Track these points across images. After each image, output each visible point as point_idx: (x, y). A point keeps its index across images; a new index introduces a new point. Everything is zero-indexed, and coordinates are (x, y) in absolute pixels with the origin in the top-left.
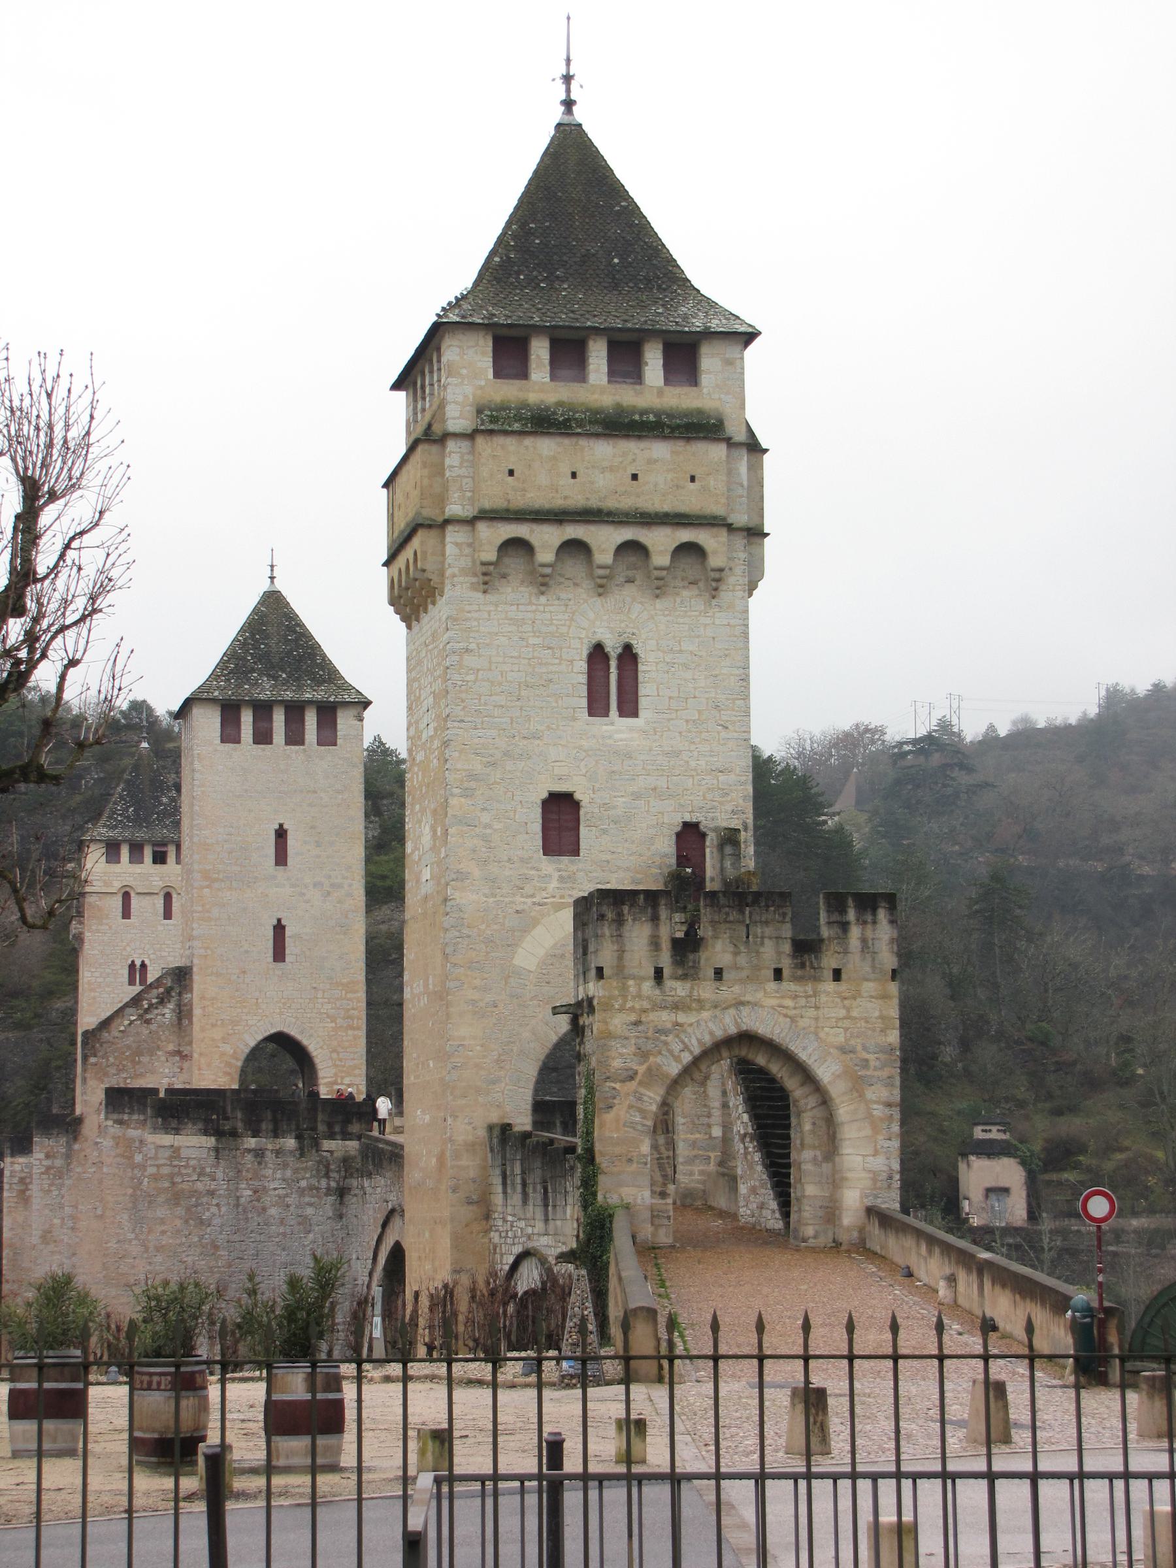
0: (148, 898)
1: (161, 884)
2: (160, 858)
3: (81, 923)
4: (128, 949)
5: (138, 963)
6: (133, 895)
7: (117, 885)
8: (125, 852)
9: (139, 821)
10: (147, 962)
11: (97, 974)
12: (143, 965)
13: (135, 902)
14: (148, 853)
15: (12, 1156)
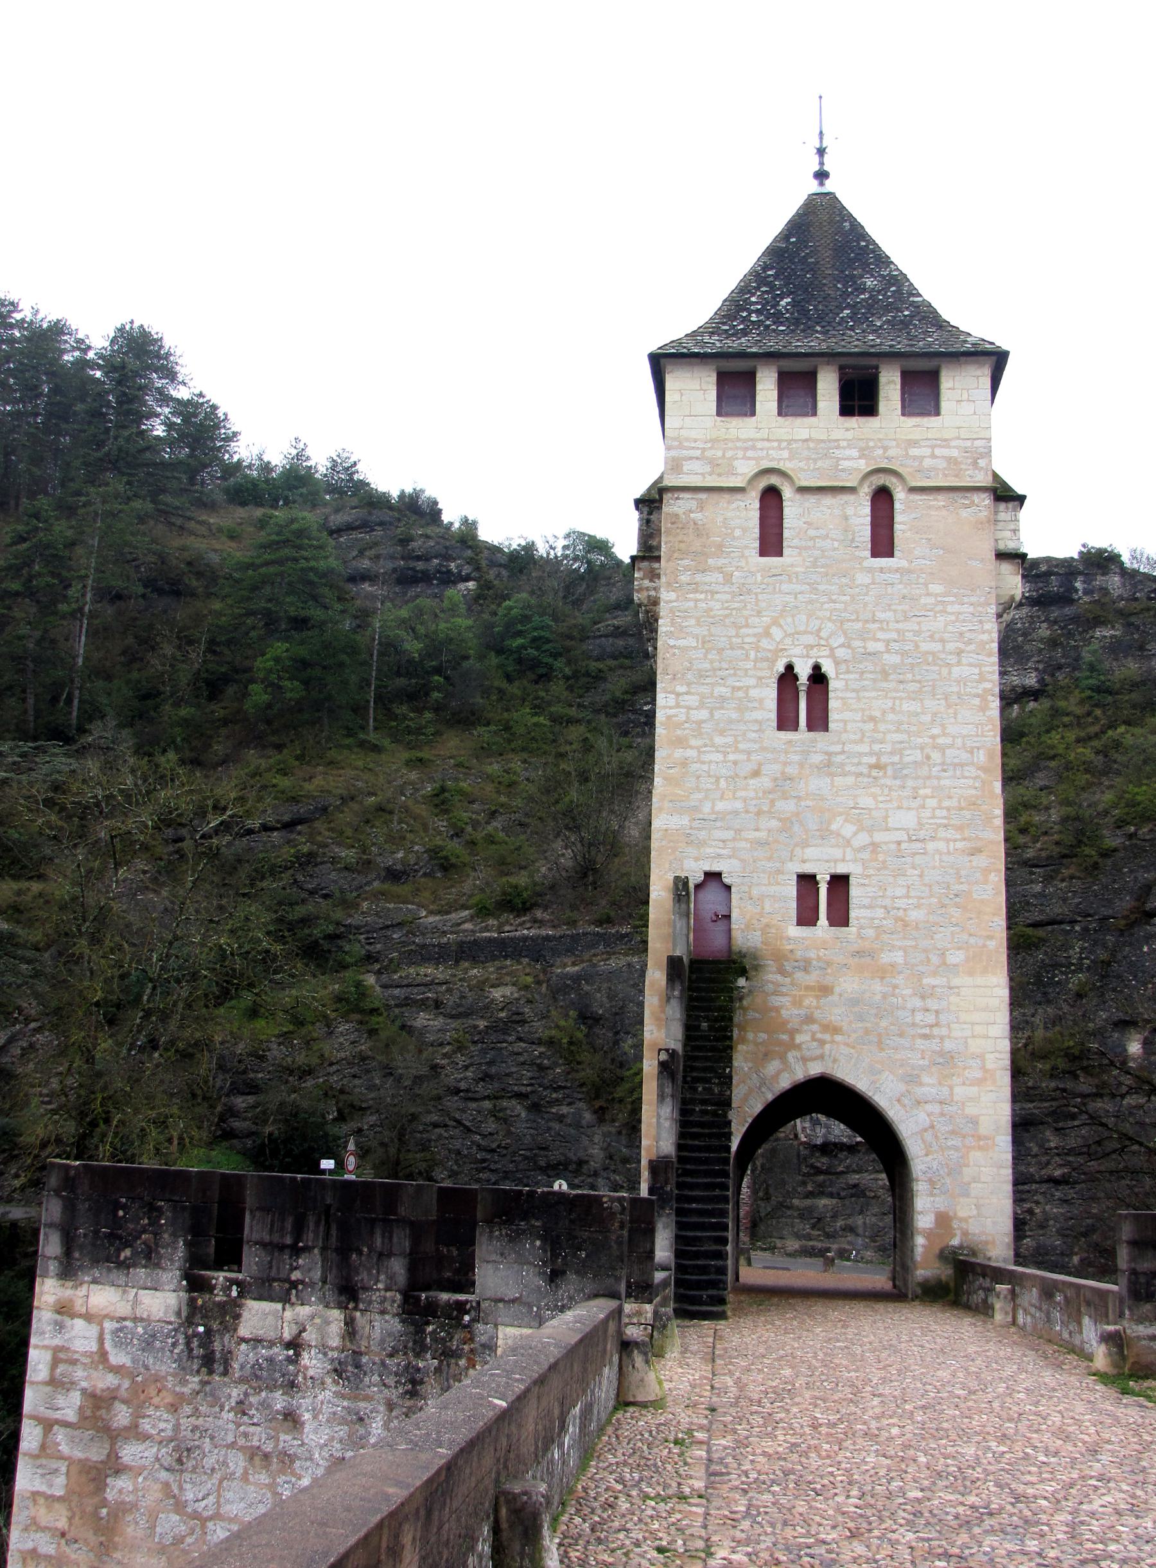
0: (828, 500)
1: (864, 466)
2: (859, 399)
3: (654, 575)
4: (777, 634)
5: (803, 672)
6: (787, 493)
7: (744, 470)
8: (767, 387)
9: (801, 320)
10: (828, 668)
11: (692, 700)
12: (818, 677)
13: (793, 509)
14: (828, 387)
15: (67, 1272)
